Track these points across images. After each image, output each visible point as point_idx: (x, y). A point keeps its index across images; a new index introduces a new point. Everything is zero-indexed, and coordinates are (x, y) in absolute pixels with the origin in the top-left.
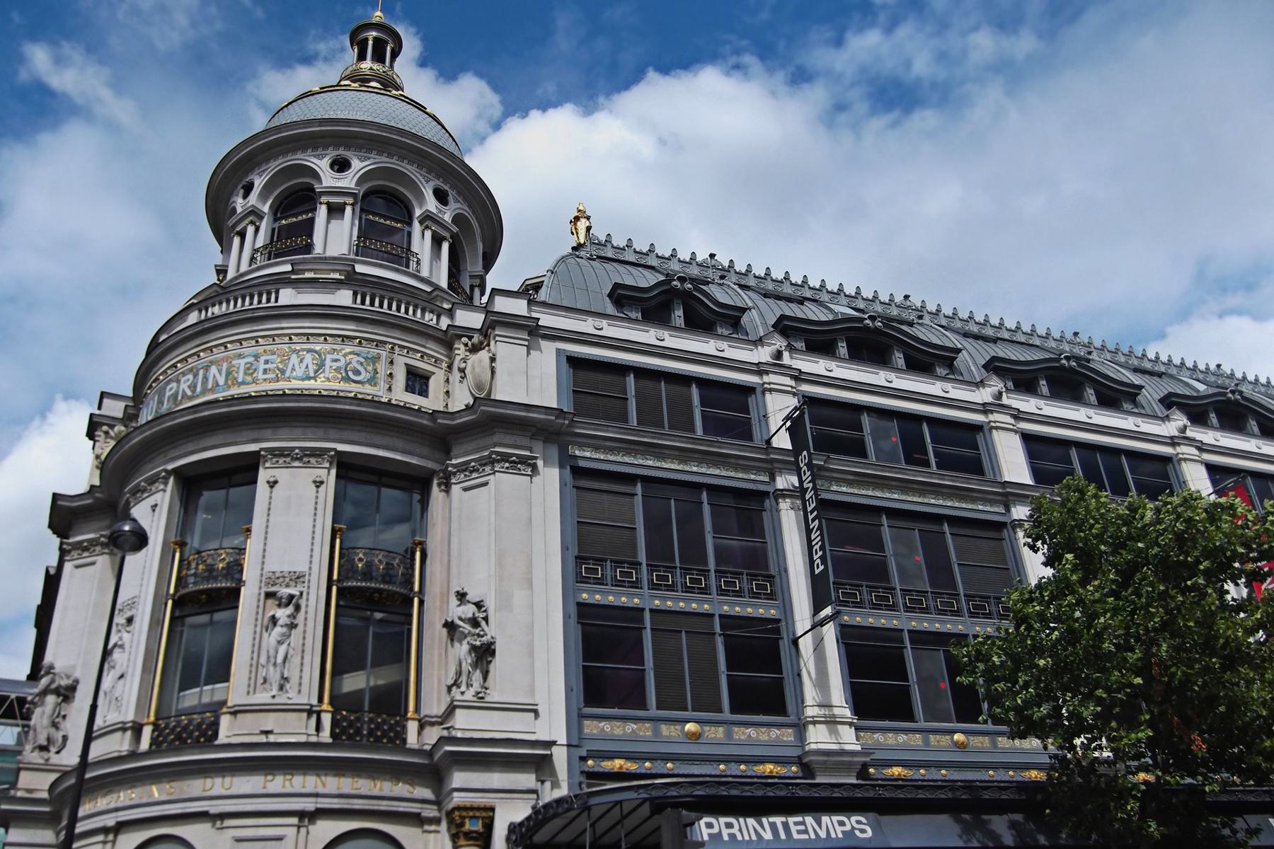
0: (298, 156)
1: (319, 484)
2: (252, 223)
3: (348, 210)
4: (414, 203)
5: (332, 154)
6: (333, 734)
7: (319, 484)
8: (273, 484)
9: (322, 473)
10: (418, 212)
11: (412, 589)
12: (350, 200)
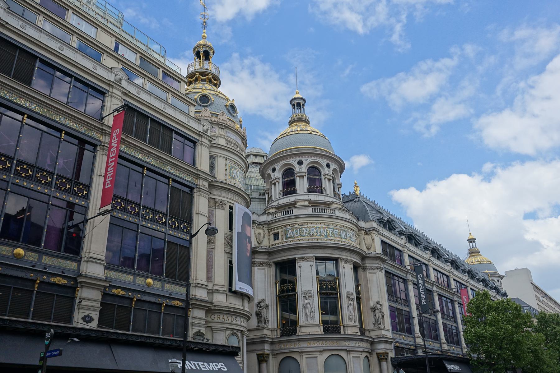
0: (288, 160)
1: (311, 266)
2: (277, 181)
3: (304, 177)
4: (320, 168)
5: (298, 159)
6: (324, 331)
7: (311, 266)
8: (300, 267)
9: (312, 263)
10: (323, 173)
11: (337, 291)
12: (304, 174)
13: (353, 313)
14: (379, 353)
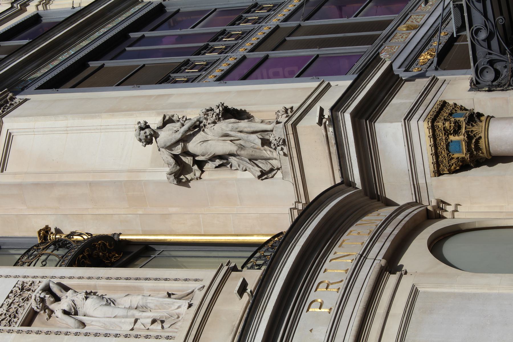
13: (125, 302)
14: (436, 154)
